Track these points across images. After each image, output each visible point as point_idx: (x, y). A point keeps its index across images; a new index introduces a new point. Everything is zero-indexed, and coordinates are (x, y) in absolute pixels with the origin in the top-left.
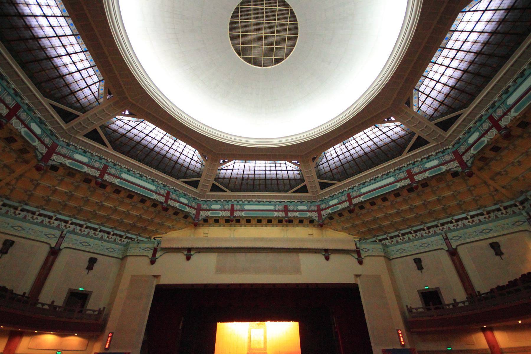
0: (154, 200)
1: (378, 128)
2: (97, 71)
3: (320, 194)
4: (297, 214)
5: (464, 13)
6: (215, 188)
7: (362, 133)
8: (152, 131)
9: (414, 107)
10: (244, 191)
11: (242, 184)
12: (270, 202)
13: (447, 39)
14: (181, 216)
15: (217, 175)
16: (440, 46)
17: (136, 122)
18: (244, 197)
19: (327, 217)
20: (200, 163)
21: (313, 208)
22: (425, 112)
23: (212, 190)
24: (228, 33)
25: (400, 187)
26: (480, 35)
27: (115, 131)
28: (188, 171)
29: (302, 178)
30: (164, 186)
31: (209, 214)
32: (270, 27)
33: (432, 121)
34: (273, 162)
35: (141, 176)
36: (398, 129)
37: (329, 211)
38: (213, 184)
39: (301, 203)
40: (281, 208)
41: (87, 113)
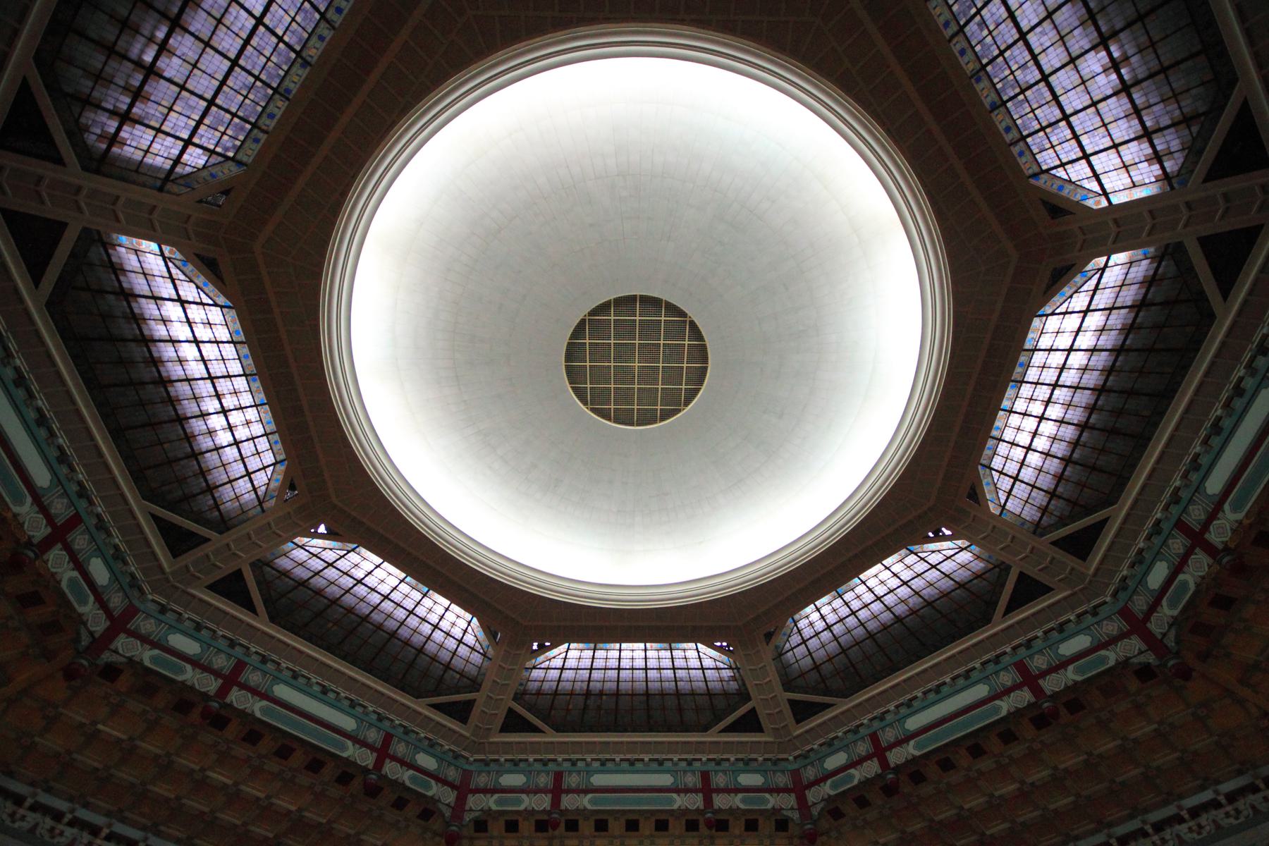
0: (347, 762)
1: (916, 554)
2: (276, 442)
4: (737, 801)
5: (1044, 318)
6: (514, 723)
7: (879, 567)
8: (372, 571)
9: (991, 506)
11: (586, 707)
12: (661, 763)
13: (1021, 365)
14: (412, 810)
15: (521, 684)
16: (1013, 378)
17: (338, 552)
18: (591, 747)
19: (822, 809)
20: (481, 651)
21: (782, 780)
22: (1019, 516)
23: (505, 729)
24: (564, 363)
25: (1009, 714)
26: (1091, 355)
27: (286, 574)
29: (743, 688)
30: (381, 718)
31: (492, 802)
32: (650, 352)
33: (1042, 535)
34: (666, 645)
35: (325, 691)
36: (965, 557)
37: (827, 789)
38: (510, 711)
39: (748, 765)
40: (692, 780)
41: (230, 532)
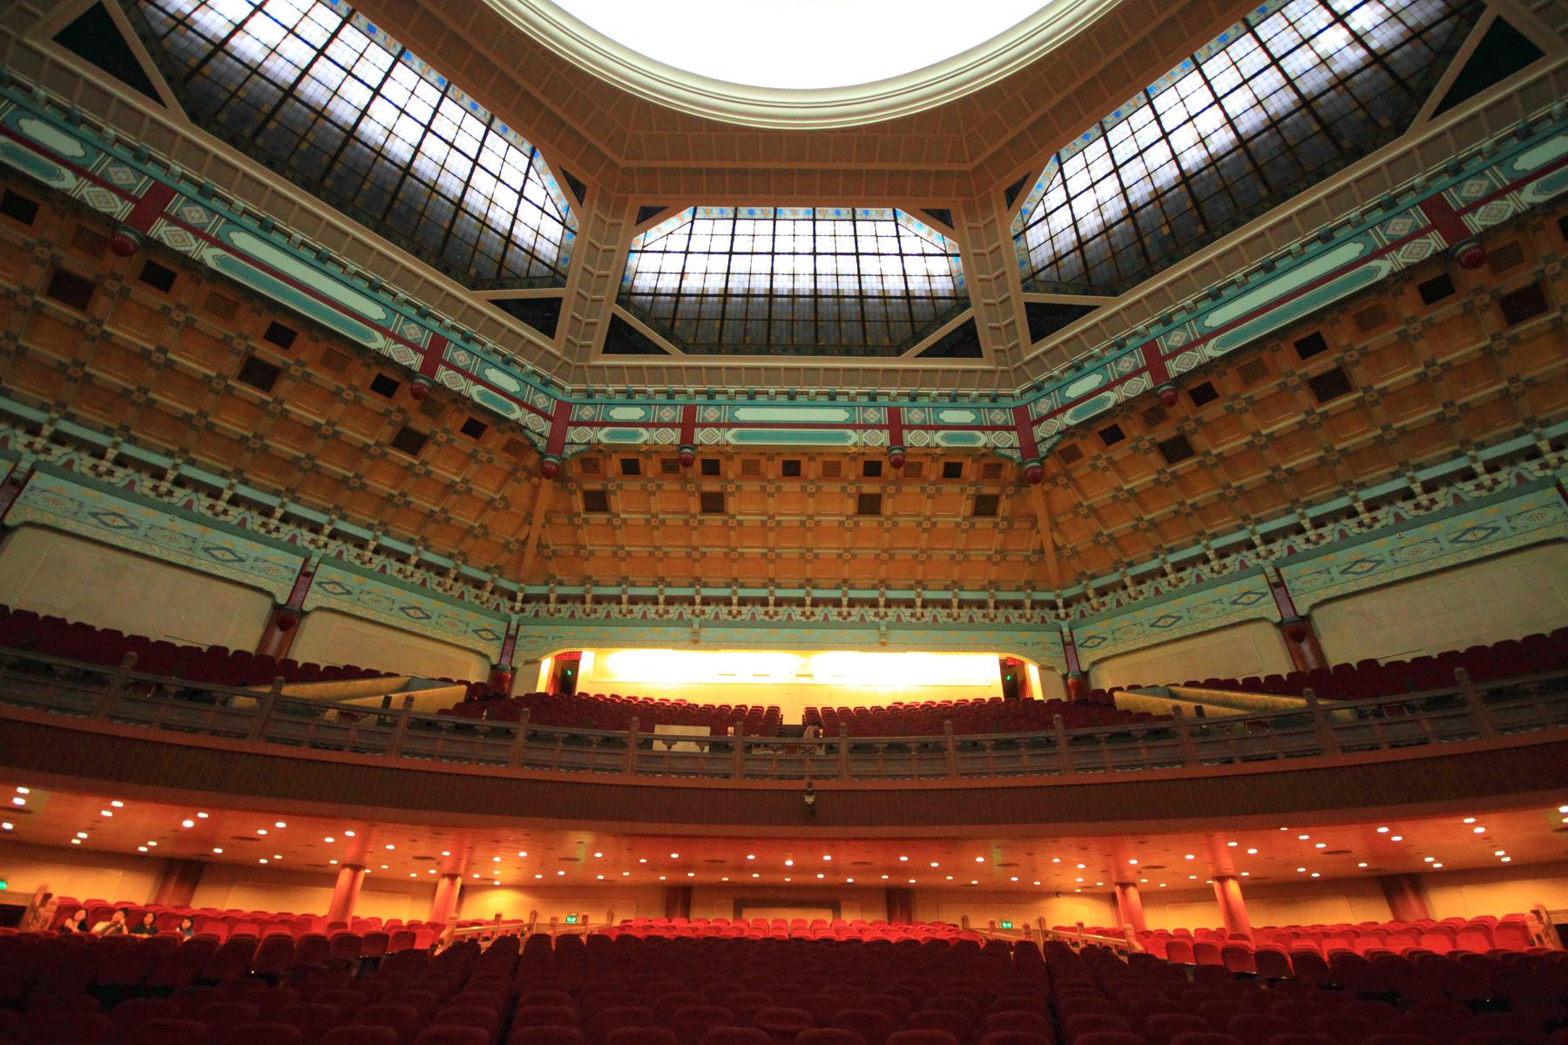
3: (1027, 364)
6: (621, 339)
10: (736, 350)
23: (607, 350)
28: (514, 255)
31: (602, 435)
37: (1068, 419)
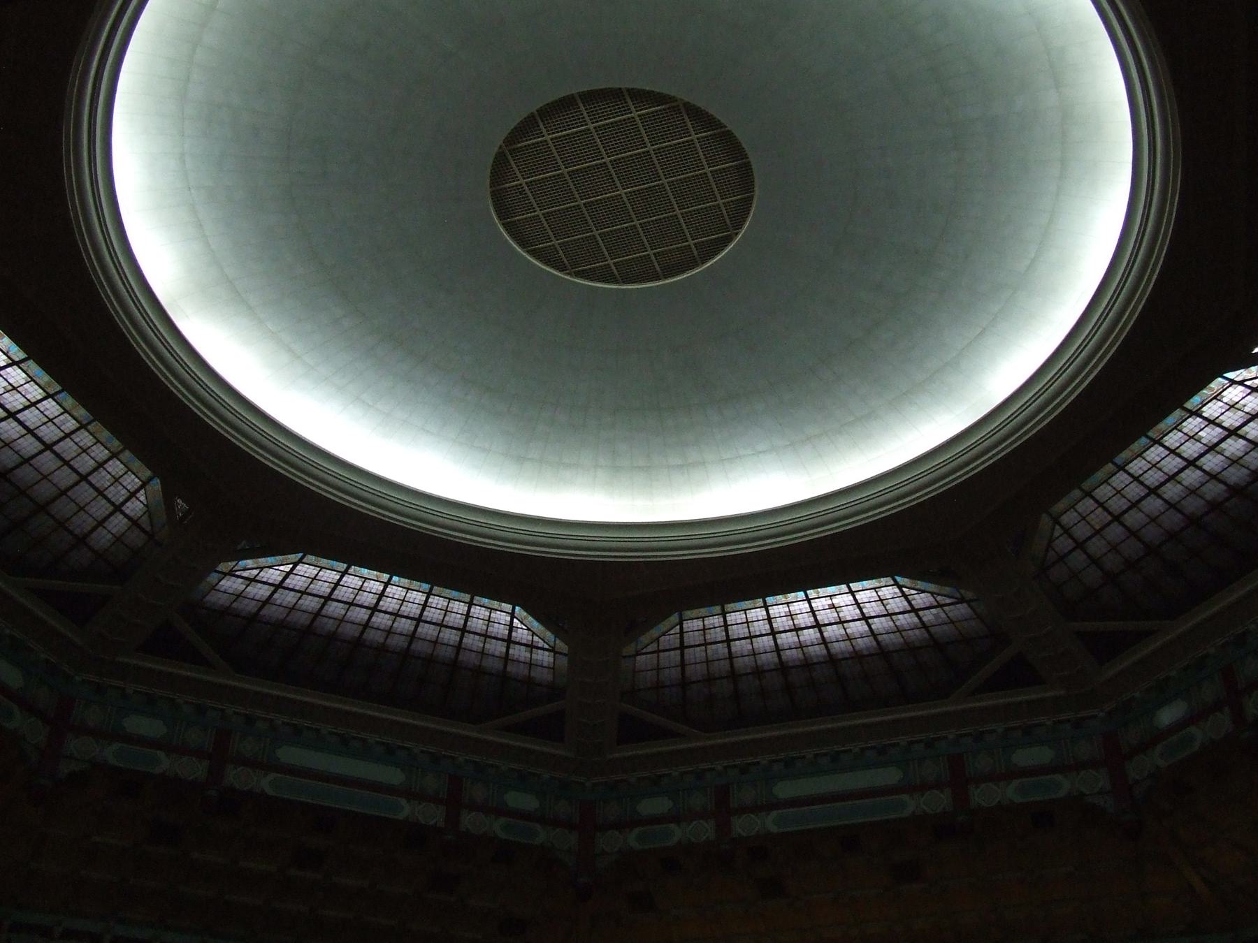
17: (282, 568)
27: (225, 612)
